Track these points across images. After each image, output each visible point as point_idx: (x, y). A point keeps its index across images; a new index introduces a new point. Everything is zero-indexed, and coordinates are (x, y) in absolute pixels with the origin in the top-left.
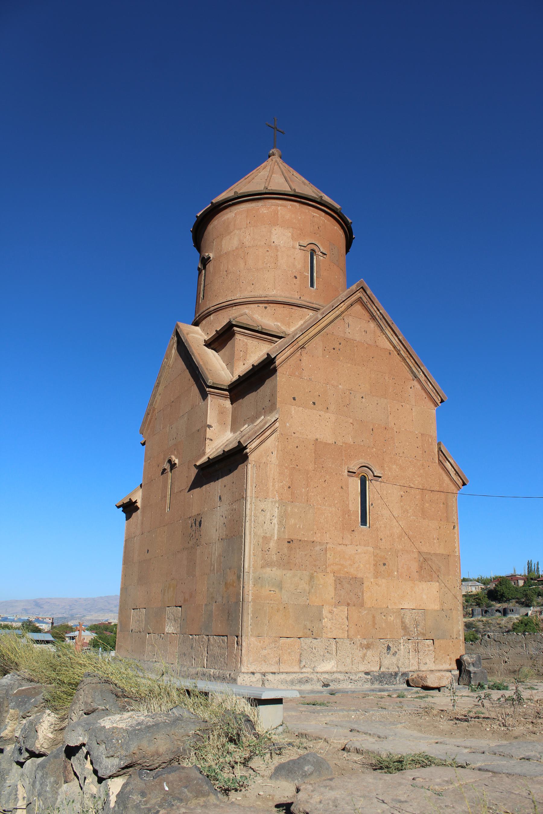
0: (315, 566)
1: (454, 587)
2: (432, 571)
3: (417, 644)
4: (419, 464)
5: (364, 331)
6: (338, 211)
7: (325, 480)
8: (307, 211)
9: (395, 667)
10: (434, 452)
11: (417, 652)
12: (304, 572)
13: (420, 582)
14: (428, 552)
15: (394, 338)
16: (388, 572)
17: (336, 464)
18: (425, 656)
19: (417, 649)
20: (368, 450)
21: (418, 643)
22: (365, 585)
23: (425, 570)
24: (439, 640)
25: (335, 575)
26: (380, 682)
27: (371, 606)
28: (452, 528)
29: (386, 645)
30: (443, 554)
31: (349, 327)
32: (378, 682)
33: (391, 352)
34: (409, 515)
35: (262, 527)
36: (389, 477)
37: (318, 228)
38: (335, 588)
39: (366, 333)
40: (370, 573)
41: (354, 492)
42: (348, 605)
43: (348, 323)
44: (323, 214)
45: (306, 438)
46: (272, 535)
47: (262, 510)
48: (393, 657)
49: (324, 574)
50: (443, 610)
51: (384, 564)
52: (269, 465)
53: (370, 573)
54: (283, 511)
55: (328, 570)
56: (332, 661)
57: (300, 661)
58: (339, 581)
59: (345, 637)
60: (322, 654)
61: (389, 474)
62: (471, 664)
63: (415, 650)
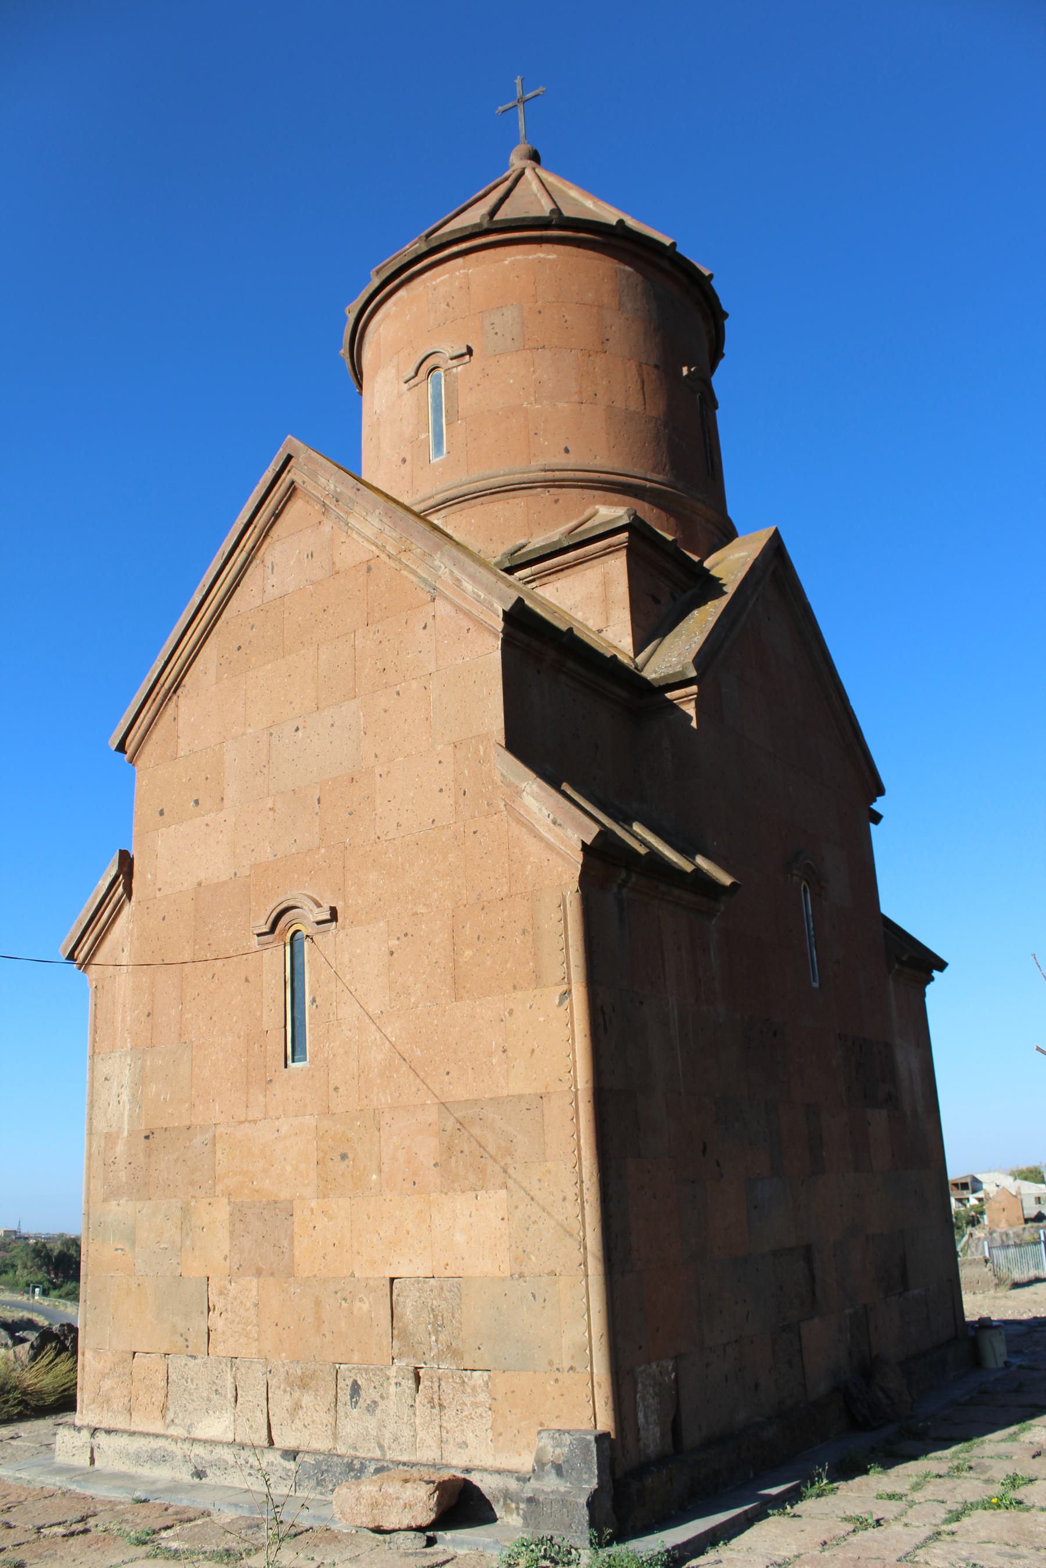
0: (192, 1183)
1: (564, 1199)
2: (485, 1155)
3: (436, 1384)
4: (444, 839)
5: (308, 556)
6: (486, 226)
7: (214, 974)
8: (421, 289)
9: (373, 1445)
10: (493, 782)
11: (438, 1408)
12: (173, 1200)
13: (446, 1194)
14: (471, 1097)
15: (370, 522)
16: (352, 1176)
17: (236, 925)
18: (461, 1420)
19: (436, 1396)
20: (308, 860)
21: (440, 1380)
22: (296, 1218)
23: (459, 1155)
24: (507, 1374)
25: (232, 1200)
26: (319, 1483)
27: (310, 1275)
28: (557, 1001)
29: (349, 1382)
30: (520, 1097)
31: (272, 573)
32: (313, 1483)
33: (372, 564)
34: (413, 1000)
35: (105, 1114)
36: (357, 912)
37: (448, 305)
38: (232, 1232)
39: (312, 556)
40: (308, 1185)
41: (273, 982)
42: (259, 1273)
43: (272, 562)
44: (459, 261)
45: (180, 891)
46: (120, 1128)
47: (106, 1079)
48: (367, 1417)
49: (209, 1200)
50: (521, 1276)
51: (344, 1157)
52: (117, 978)
53: (308, 1185)
54: (138, 1071)
55: (219, 1188)
56: (225, 1415)
57: (164, 1409)
58: (238, 1215)
59: (253, 1356)
60: (205, 1394)
61: (360, 902)
62: (548, 1467)
63: (431, 1400)
